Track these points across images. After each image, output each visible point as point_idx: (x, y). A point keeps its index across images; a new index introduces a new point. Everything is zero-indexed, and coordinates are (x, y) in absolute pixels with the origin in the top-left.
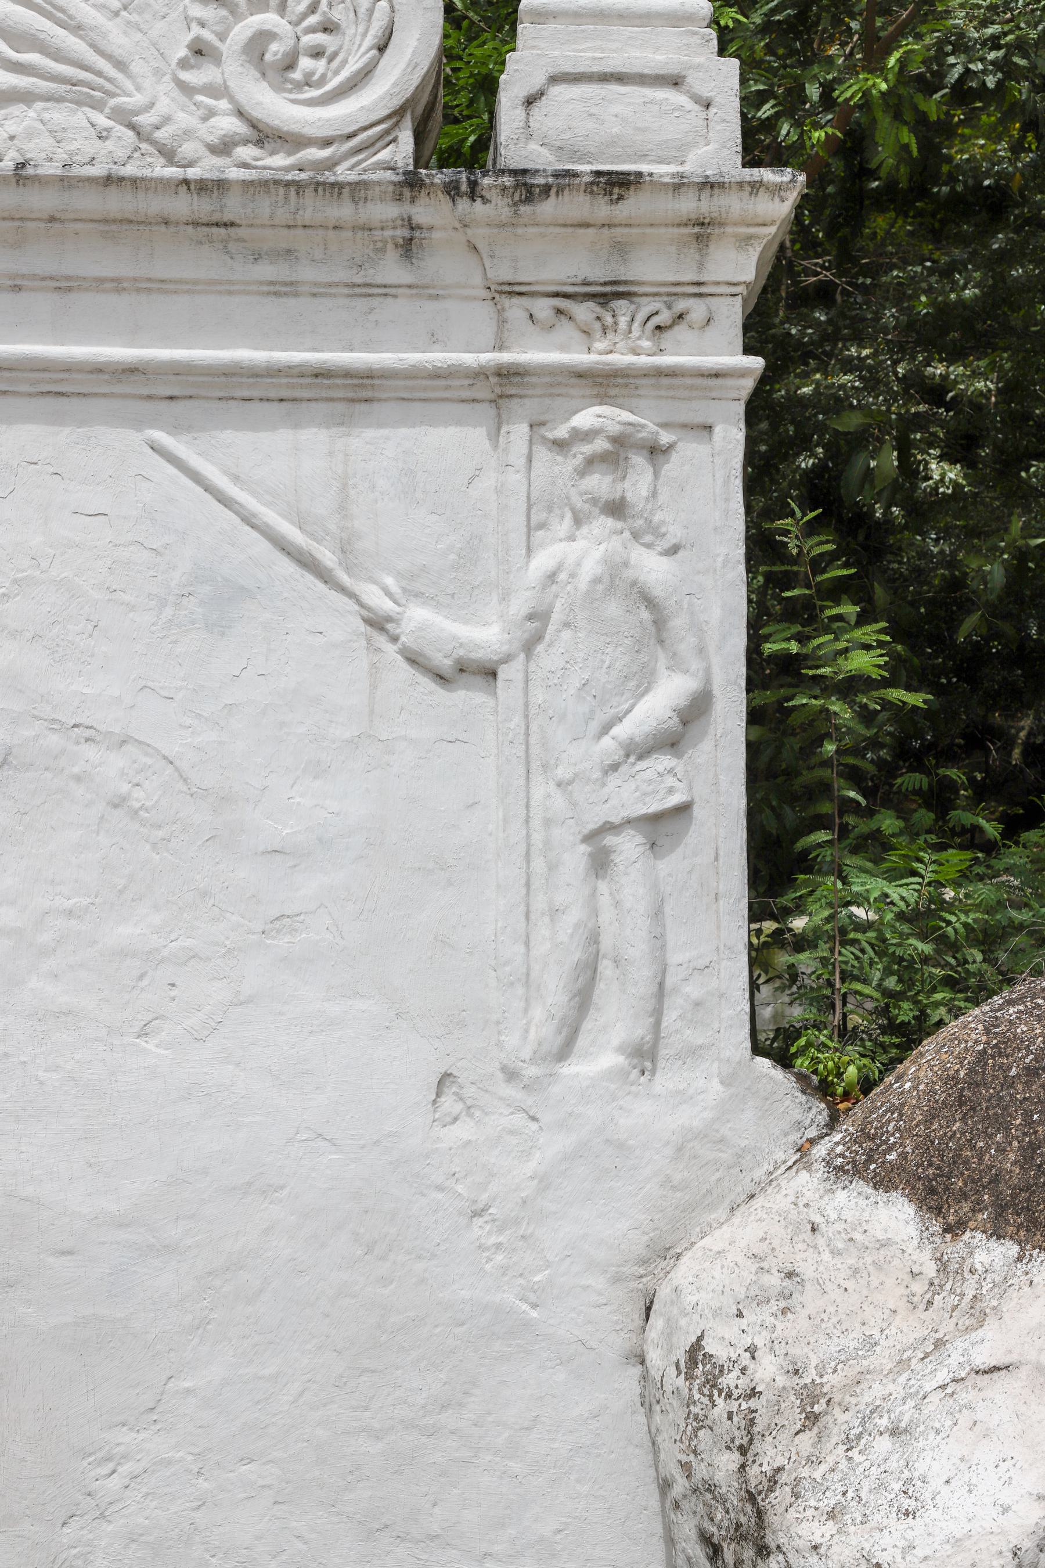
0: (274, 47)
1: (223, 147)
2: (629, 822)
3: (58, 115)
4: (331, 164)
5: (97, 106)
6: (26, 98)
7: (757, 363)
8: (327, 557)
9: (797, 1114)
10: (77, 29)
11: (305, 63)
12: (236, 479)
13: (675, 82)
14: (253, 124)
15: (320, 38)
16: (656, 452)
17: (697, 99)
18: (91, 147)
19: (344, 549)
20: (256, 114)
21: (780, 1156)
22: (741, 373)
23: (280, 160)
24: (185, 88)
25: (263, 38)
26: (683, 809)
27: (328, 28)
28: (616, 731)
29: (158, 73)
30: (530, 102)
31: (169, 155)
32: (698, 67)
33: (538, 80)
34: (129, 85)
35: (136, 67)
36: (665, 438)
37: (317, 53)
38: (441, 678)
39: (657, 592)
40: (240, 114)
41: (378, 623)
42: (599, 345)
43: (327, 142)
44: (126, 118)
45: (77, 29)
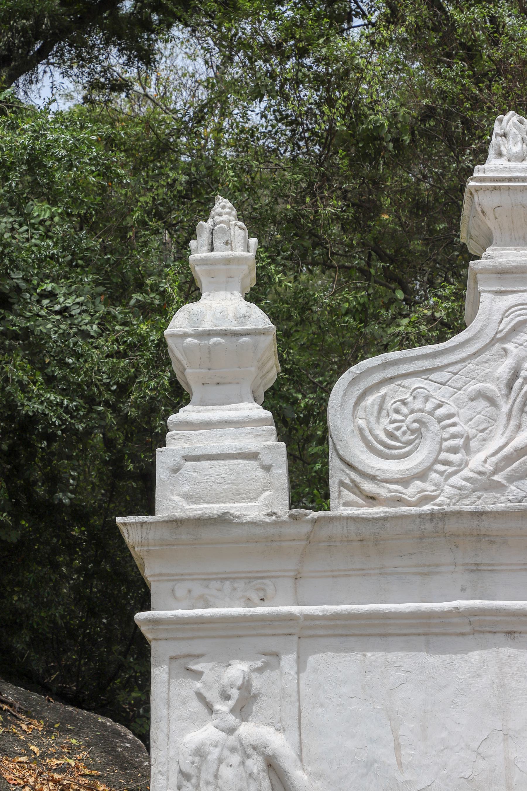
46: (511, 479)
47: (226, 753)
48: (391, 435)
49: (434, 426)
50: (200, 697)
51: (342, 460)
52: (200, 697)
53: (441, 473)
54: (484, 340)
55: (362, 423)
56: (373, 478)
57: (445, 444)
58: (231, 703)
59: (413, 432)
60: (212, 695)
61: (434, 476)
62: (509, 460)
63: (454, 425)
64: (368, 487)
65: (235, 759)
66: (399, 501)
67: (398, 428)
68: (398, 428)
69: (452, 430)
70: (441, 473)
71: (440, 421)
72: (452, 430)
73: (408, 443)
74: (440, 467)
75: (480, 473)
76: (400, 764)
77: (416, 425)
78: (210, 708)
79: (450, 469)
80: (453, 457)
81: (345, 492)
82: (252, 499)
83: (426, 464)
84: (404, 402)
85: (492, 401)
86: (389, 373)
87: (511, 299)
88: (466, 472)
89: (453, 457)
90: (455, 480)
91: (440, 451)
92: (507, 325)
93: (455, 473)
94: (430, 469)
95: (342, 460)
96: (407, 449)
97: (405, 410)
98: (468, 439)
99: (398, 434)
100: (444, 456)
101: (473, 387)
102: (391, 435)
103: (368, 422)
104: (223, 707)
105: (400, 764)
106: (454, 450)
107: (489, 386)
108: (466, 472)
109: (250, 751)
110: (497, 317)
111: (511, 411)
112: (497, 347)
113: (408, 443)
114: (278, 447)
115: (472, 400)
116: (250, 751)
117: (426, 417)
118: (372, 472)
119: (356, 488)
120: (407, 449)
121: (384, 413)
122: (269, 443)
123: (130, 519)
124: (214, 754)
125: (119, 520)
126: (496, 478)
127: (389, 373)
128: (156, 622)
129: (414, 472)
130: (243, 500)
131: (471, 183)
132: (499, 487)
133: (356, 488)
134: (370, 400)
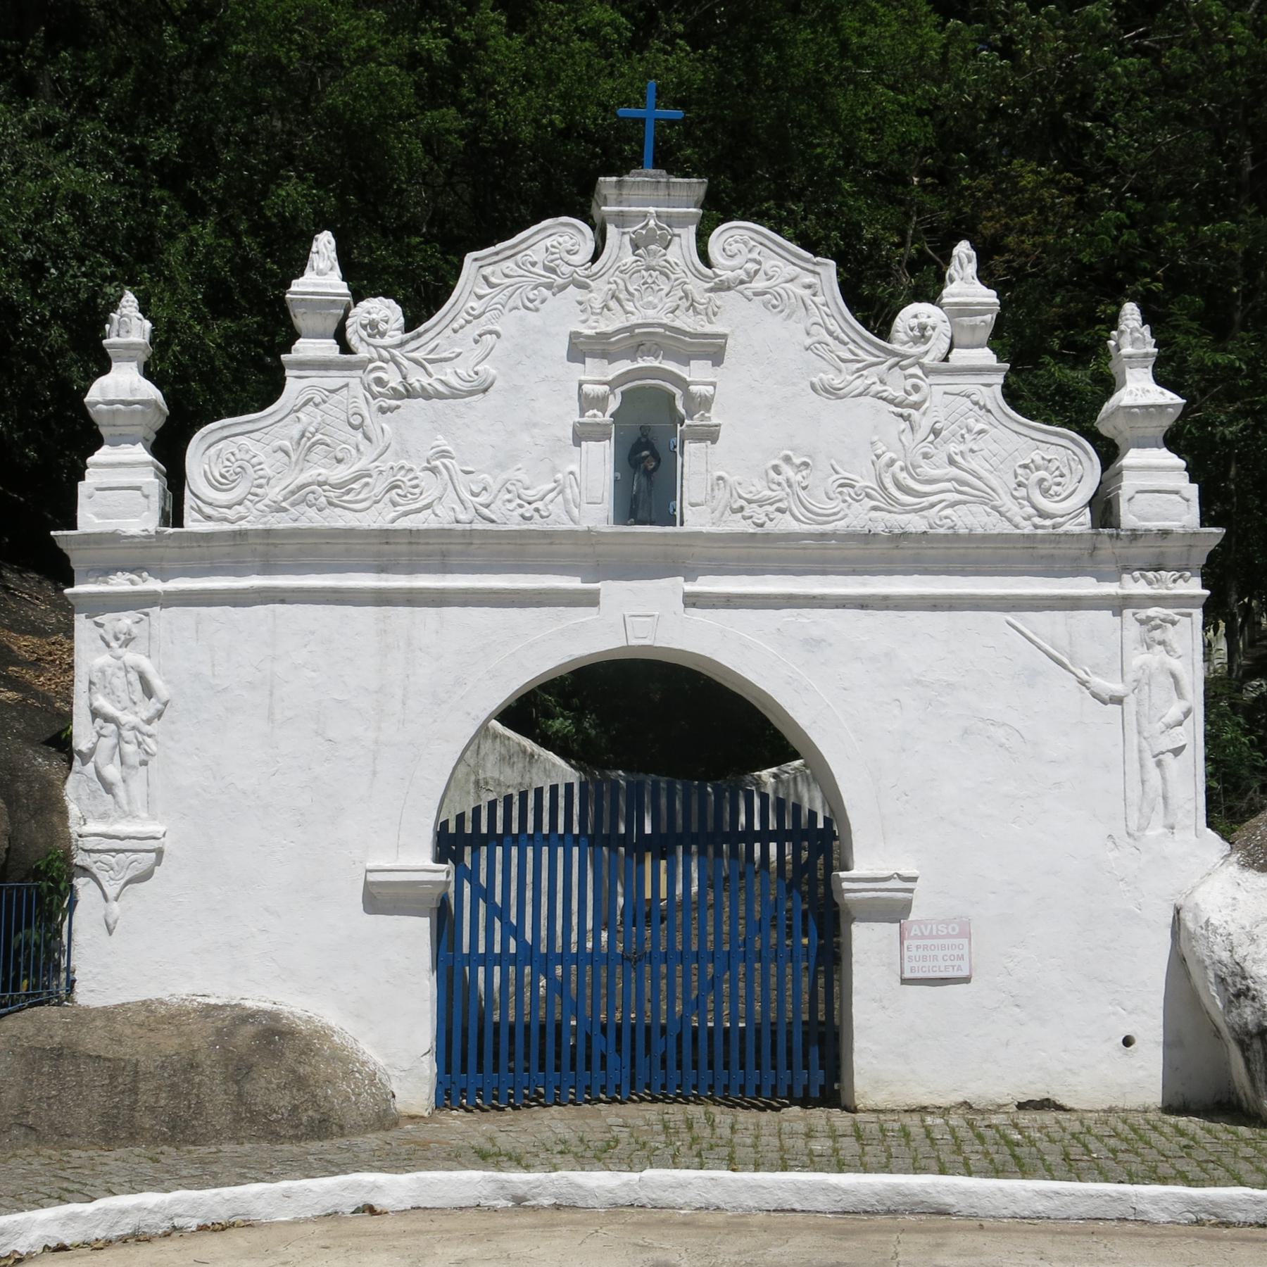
0: (1045, 483)
1: (1028, 518)
2: (1168, 751)
3: (974, 508)
4: (1061, 525)
5: (986, 504)
6: (965, 503)
7: (1207, 592)
8: (1066, 661)
9: (1221, 847)
10: (980, 478)
11: (1055, 488)
12: (1035, 633)
13: (1177, 493)
14: (1037, 510)
15: (1059, 479)
16: (1174, 623)
17: (1184, 499)
18: (985, 519)
19: (1071, 659)
20: (1040, 506)
21: (1216, 861)
22: (1202, 596)
23: (1048, 522)
24: (1015, 498)
25: (1042, 480)
26: (1184, 747)
27: (1062, 476)
28: (1163, 720)
29: (1006, 493)
30: (1130, 500)
31: (1010, 520)
32: (1185, 487)
33: (1131, 493)
34: (997, 498)
35: (1000, 491)
36: (1177, 618)
37: (1059, 484)
38: (1104, 702)
39: (1177, 673)
40: (1034, 507)
41: (1083, 683)
42: (1155, 586)
43: (1062, 516)
44: (994, 508)
45: (980, 478)
46: (293, 505)
47: (116, 670)
48: (223, 476)
49: (250, 470)
50: (103, 638)
51: (192, 492)
52: (103, 638)
53: (251, 501)
54: (286, 412)
55: (206, 467)
56: (210, 504)
57: (256, 482)
58: (120, 642)
59: (237, 474)
60: (109, 638)
61: (247, 502)
62: (293, 493)
63: (262, 469)
64: (207, 510)
65: (122, 674)
66: (225, 520)
67: (228, 471)
68: (228, 471)
69: (261, 473)
70: (251, 501)
71: (253, 466)
72: (261, 473)
73: (233, 481)
74: (250, 497)
75: (274, 502)
76: (214, 675)
77: (239, 470)
78: (108, 645)
79: (257, 499)
80: (259, 491)
81: (194, 513)
82: (136, 517)
83: (243, 496)
84: (233, 454)
85: (287, 453)
86: (226, 433)
87: (305, 382)
88: (266, 501)
89: (259, 491)
90: (260, 506)
91: (252, 486)
92: (300, 401)
93: (259, 501)
94: (245, 498)
95: (192, 492)
96: (233, 485)
97: (233, 459)
98: (269, 479)
99: (227, 475)
100: (254, 490)
101: (277, 443)
102: (223, 476)
103: (210, 467)
104: (114, 644)
105: (214, 675)
106: (260, 486)
107: (287, 443)
108: (266, 501)
109: (130, 669)
110: (295, 395)
111: (298, 460)
112: (293, 416)
113: (233, 481)
114: (153, 483)
115: (275, 452)
116: (130, 669)
117: (245, 464)
118: (210, 501)
119: (200, 511)
120: (233, 485)
121: (220, 460)
122: (148, 480)
123: (59, 533)
124: (109, 671)
125: (52, 533)
126: (284, 504)
127: (226, 433)
128: (76, 595)
129: (235, 501)
130: (132, 517)
131: (288, 296)
132: (285, 510)
133: (200, 511)
134: (213, 450)
